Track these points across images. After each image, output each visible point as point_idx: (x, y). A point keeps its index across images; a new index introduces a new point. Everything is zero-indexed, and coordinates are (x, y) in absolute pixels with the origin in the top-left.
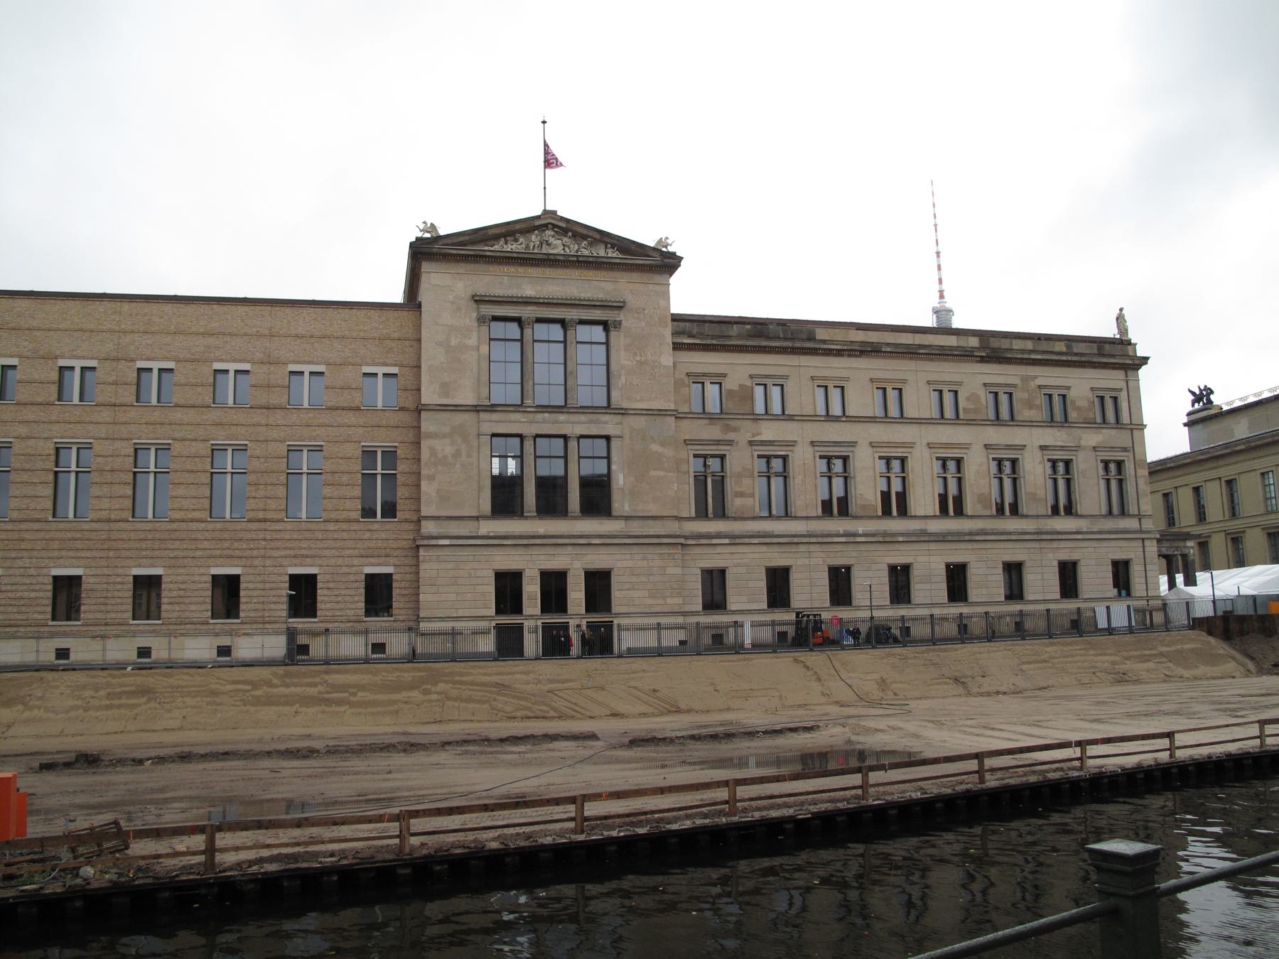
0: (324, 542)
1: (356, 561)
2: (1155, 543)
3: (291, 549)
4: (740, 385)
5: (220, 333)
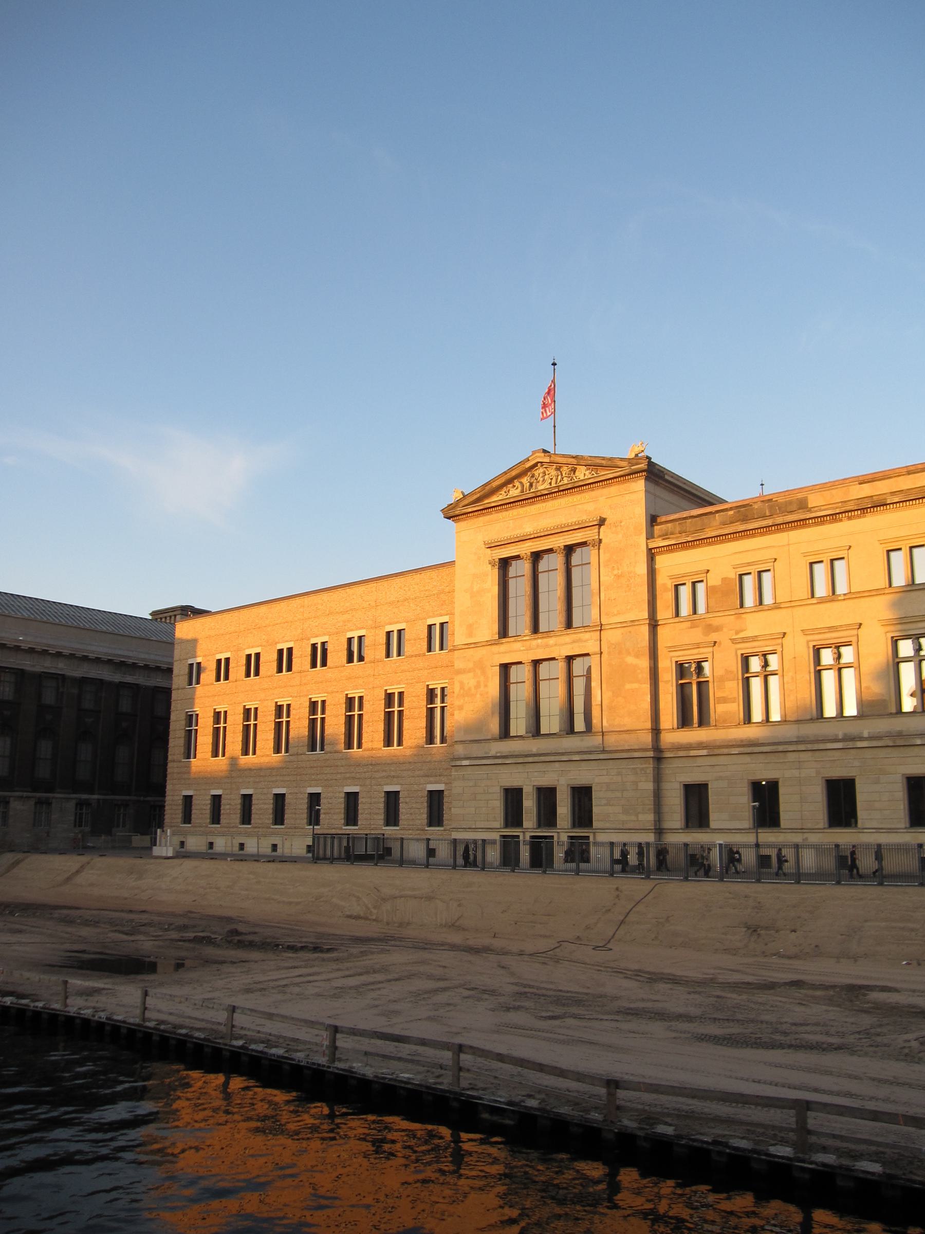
0: (404, 765)
1: (422, 780)
3: (385, 771)
5: (351, 610)
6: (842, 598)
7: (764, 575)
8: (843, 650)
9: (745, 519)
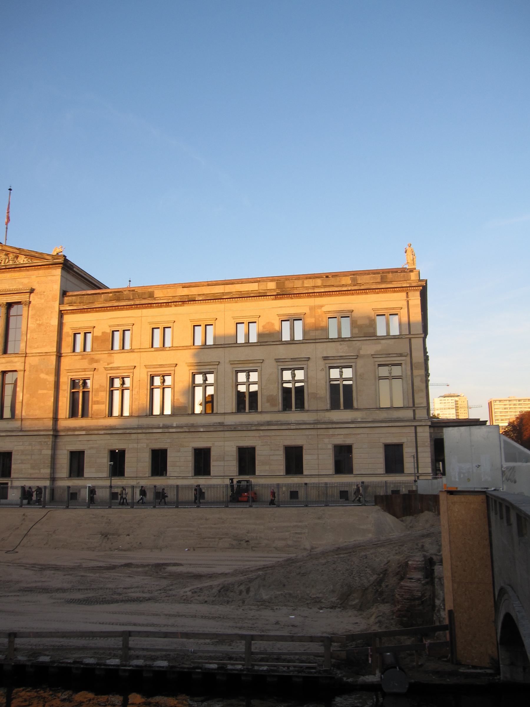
2: (428, 427)
4: (103, 333)
6: (168, 349)
7: (126, 332)
8: (166, 378)
9: (118, 299)
